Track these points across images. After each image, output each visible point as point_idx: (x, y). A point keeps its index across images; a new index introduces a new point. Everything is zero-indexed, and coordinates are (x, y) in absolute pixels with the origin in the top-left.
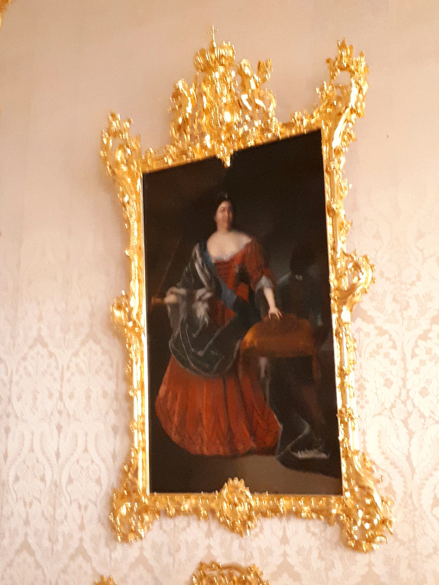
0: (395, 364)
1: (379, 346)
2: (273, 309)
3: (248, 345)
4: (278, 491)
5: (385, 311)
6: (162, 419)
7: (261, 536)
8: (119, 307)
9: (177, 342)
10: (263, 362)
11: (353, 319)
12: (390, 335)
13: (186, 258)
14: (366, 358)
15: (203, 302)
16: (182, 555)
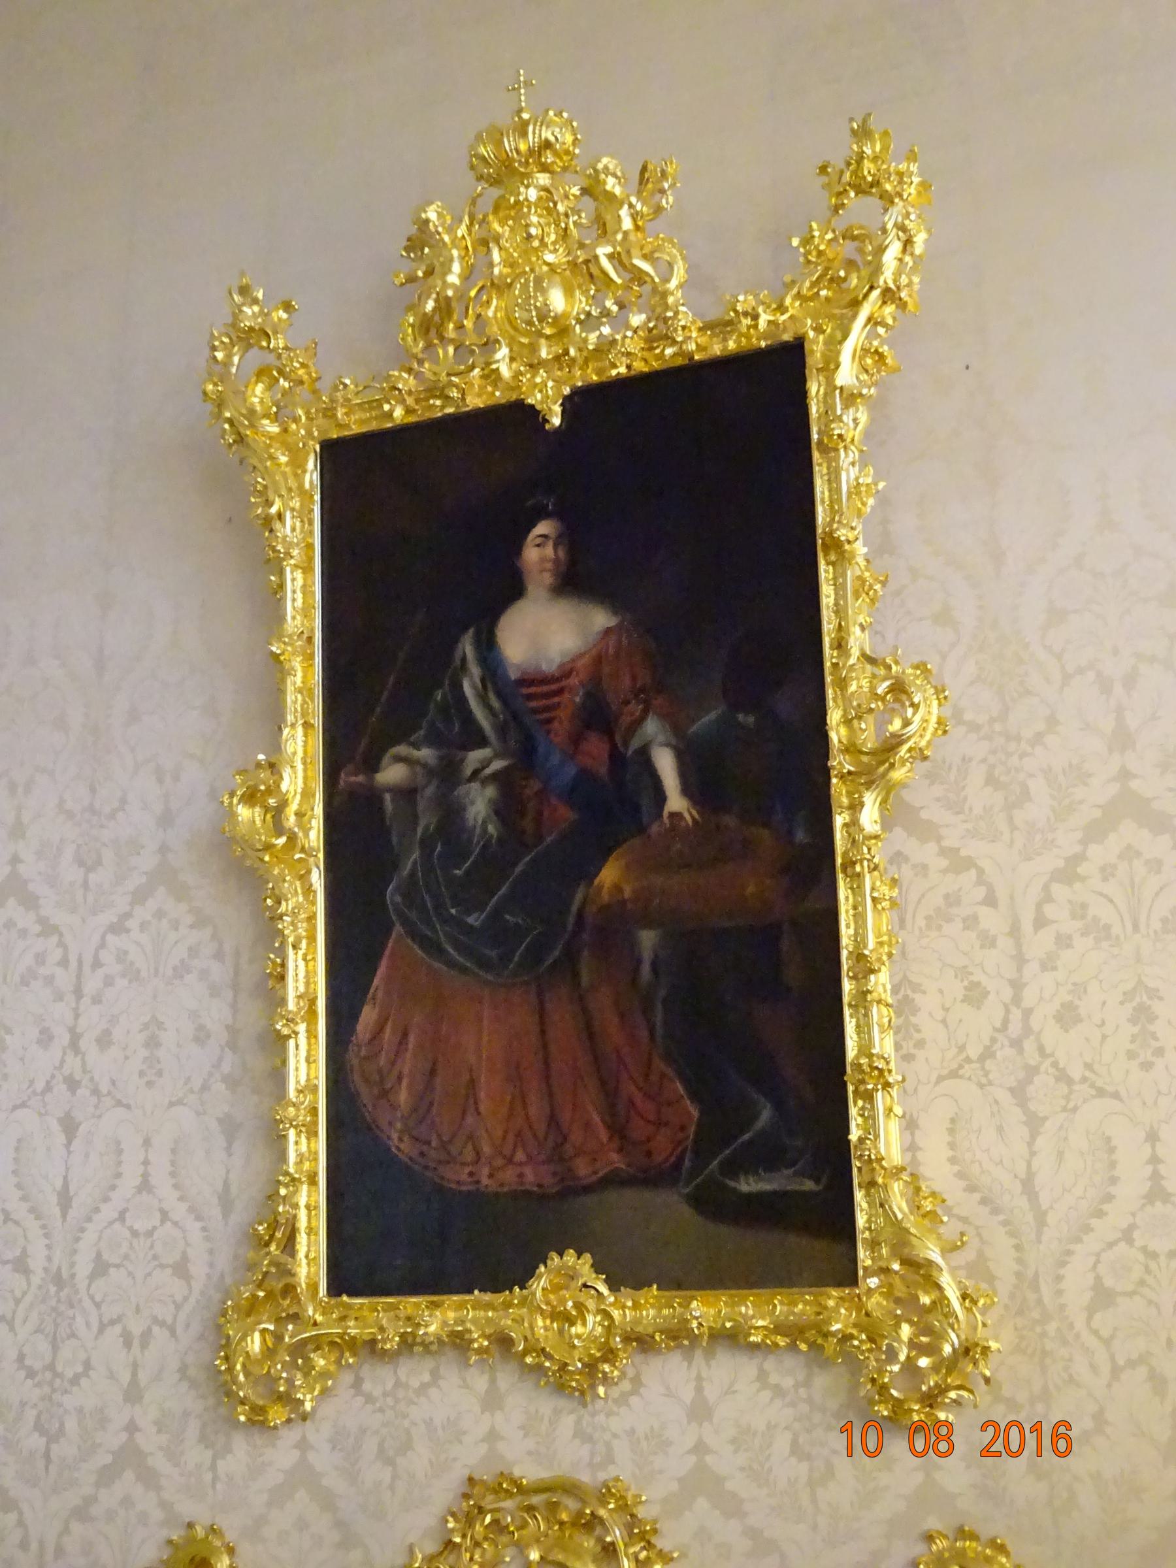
0: (993, 944)
1: (952, 900)
2: (676, 802)
3: (605, 897)
4: (680, 1280)
5: (967, 811)
6: (366, 1095)
7: (634, 1400)
9: (410, 891)
10: (648, 939)
11: (887, 823)
12: (981, 872)
13: (438, 663)
14: (917, 932)
15: (484, 782)
16: (419, 1460)
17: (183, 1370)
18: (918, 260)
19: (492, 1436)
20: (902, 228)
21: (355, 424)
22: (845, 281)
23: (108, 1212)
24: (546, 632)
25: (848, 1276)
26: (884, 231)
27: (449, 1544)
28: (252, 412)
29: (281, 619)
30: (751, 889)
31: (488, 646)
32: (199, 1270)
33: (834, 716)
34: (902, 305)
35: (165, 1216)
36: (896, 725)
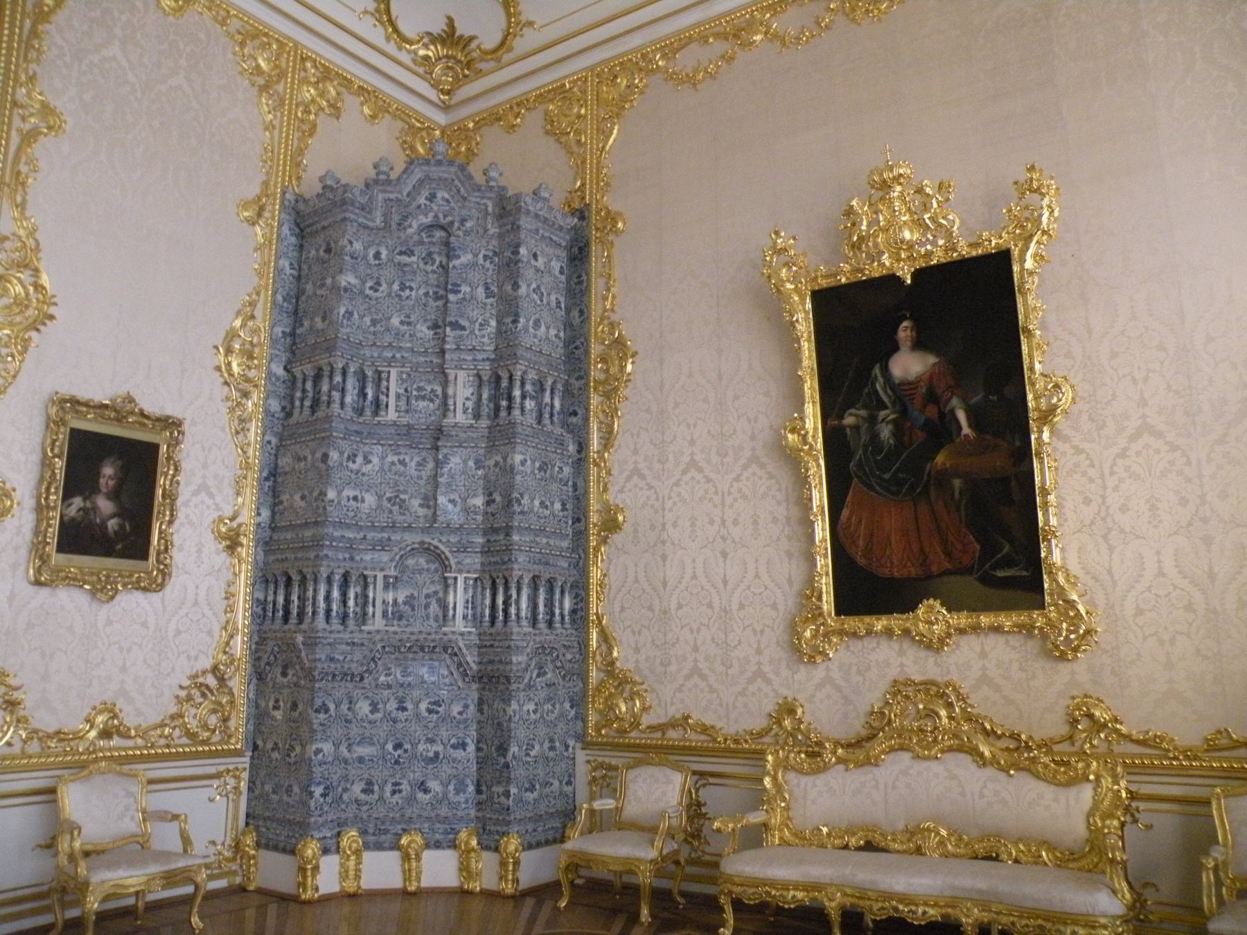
2: (966, 430)
4: (974, 609)
8: (793, 431)
9: (860, 465)
13: (864, 377)
15: (888, 423)
17: (778, 643)
18: (1056, 219)
19: (902, 665)
20: (1049, 207)
21: (824, 283)
22: (1028, 228)
23: (742, 586)
24: (909, 365)
25: (1041, 606)
26: (1042, 208)
27: (887, 703)
28: (782, 280)
29: (800, 361)
30: (998, 463)
31: (885, 370)
32: (781, 607)
33: (1030, 397)
34: (1050, 236)
35: (766, 588)
36: (1055, 400)
